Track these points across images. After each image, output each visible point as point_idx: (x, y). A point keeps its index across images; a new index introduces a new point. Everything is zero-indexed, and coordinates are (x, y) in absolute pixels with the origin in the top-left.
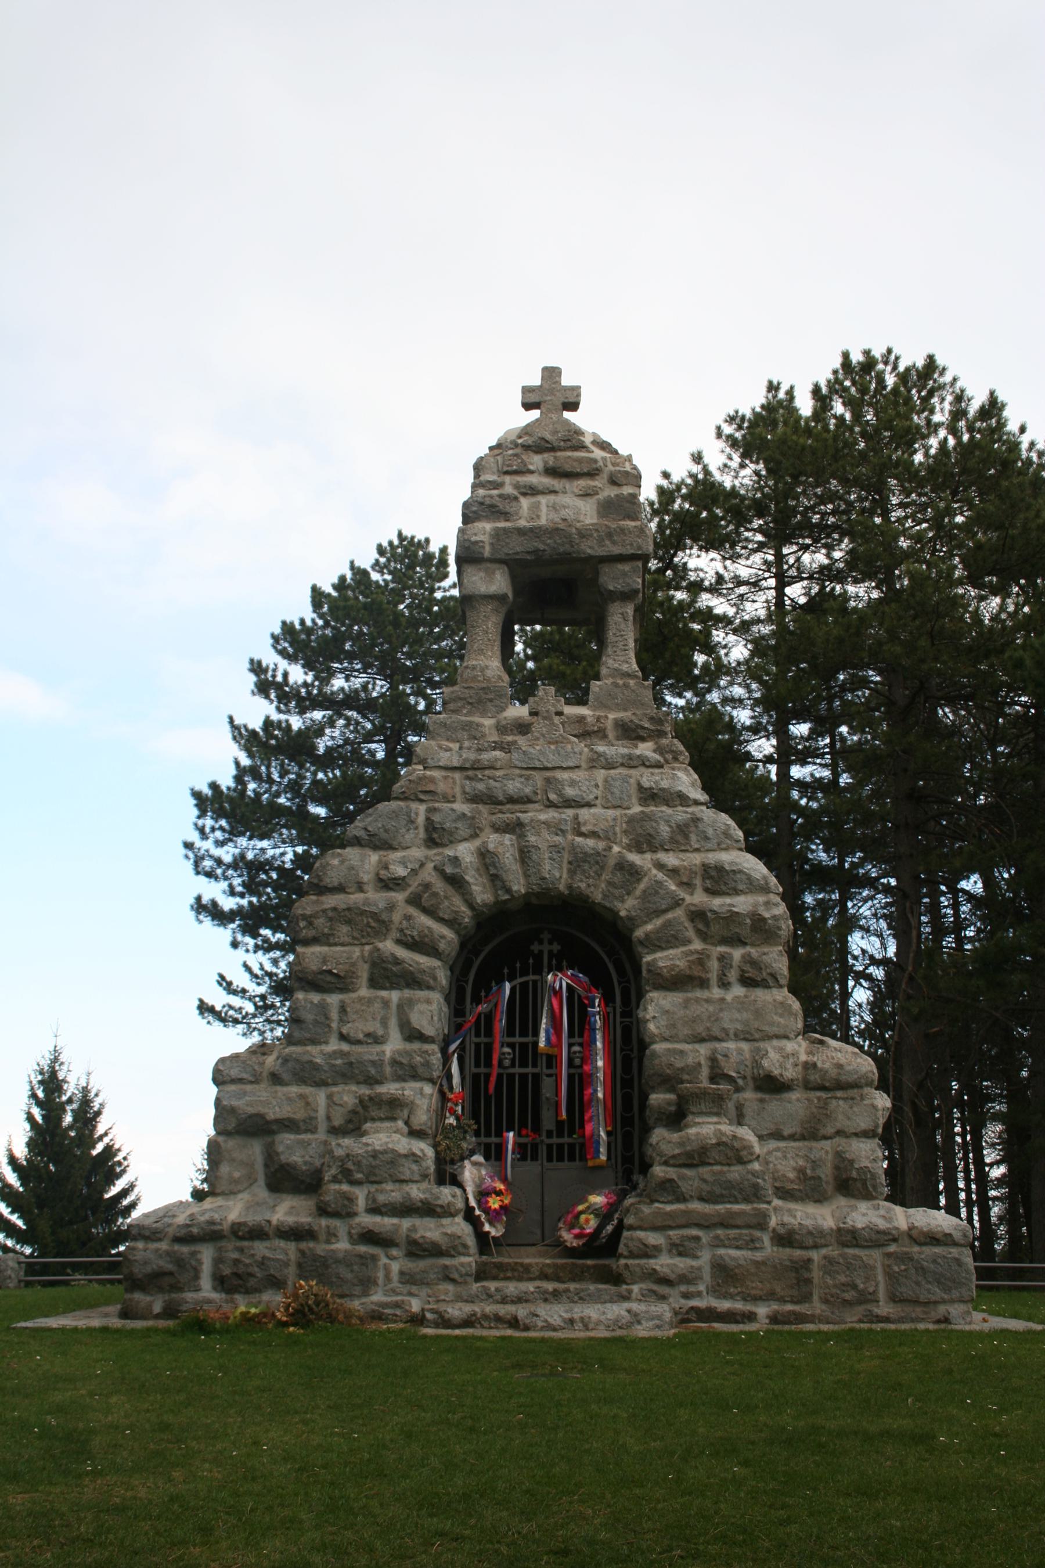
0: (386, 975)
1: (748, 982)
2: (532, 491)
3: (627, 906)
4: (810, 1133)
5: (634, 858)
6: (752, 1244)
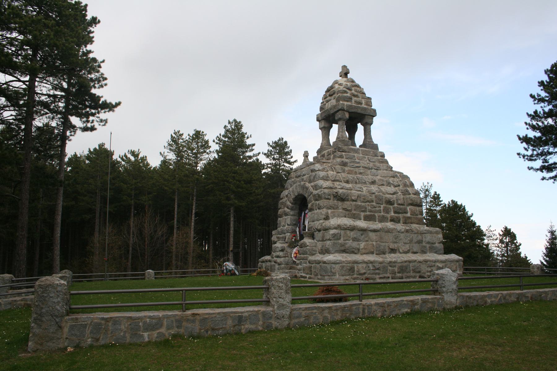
0: (286, 214)
1: (319, 209)
2: (327, 101)
3: (306, 196)
4: (323, 241)
5: (308, 185)
6: (306, 263)
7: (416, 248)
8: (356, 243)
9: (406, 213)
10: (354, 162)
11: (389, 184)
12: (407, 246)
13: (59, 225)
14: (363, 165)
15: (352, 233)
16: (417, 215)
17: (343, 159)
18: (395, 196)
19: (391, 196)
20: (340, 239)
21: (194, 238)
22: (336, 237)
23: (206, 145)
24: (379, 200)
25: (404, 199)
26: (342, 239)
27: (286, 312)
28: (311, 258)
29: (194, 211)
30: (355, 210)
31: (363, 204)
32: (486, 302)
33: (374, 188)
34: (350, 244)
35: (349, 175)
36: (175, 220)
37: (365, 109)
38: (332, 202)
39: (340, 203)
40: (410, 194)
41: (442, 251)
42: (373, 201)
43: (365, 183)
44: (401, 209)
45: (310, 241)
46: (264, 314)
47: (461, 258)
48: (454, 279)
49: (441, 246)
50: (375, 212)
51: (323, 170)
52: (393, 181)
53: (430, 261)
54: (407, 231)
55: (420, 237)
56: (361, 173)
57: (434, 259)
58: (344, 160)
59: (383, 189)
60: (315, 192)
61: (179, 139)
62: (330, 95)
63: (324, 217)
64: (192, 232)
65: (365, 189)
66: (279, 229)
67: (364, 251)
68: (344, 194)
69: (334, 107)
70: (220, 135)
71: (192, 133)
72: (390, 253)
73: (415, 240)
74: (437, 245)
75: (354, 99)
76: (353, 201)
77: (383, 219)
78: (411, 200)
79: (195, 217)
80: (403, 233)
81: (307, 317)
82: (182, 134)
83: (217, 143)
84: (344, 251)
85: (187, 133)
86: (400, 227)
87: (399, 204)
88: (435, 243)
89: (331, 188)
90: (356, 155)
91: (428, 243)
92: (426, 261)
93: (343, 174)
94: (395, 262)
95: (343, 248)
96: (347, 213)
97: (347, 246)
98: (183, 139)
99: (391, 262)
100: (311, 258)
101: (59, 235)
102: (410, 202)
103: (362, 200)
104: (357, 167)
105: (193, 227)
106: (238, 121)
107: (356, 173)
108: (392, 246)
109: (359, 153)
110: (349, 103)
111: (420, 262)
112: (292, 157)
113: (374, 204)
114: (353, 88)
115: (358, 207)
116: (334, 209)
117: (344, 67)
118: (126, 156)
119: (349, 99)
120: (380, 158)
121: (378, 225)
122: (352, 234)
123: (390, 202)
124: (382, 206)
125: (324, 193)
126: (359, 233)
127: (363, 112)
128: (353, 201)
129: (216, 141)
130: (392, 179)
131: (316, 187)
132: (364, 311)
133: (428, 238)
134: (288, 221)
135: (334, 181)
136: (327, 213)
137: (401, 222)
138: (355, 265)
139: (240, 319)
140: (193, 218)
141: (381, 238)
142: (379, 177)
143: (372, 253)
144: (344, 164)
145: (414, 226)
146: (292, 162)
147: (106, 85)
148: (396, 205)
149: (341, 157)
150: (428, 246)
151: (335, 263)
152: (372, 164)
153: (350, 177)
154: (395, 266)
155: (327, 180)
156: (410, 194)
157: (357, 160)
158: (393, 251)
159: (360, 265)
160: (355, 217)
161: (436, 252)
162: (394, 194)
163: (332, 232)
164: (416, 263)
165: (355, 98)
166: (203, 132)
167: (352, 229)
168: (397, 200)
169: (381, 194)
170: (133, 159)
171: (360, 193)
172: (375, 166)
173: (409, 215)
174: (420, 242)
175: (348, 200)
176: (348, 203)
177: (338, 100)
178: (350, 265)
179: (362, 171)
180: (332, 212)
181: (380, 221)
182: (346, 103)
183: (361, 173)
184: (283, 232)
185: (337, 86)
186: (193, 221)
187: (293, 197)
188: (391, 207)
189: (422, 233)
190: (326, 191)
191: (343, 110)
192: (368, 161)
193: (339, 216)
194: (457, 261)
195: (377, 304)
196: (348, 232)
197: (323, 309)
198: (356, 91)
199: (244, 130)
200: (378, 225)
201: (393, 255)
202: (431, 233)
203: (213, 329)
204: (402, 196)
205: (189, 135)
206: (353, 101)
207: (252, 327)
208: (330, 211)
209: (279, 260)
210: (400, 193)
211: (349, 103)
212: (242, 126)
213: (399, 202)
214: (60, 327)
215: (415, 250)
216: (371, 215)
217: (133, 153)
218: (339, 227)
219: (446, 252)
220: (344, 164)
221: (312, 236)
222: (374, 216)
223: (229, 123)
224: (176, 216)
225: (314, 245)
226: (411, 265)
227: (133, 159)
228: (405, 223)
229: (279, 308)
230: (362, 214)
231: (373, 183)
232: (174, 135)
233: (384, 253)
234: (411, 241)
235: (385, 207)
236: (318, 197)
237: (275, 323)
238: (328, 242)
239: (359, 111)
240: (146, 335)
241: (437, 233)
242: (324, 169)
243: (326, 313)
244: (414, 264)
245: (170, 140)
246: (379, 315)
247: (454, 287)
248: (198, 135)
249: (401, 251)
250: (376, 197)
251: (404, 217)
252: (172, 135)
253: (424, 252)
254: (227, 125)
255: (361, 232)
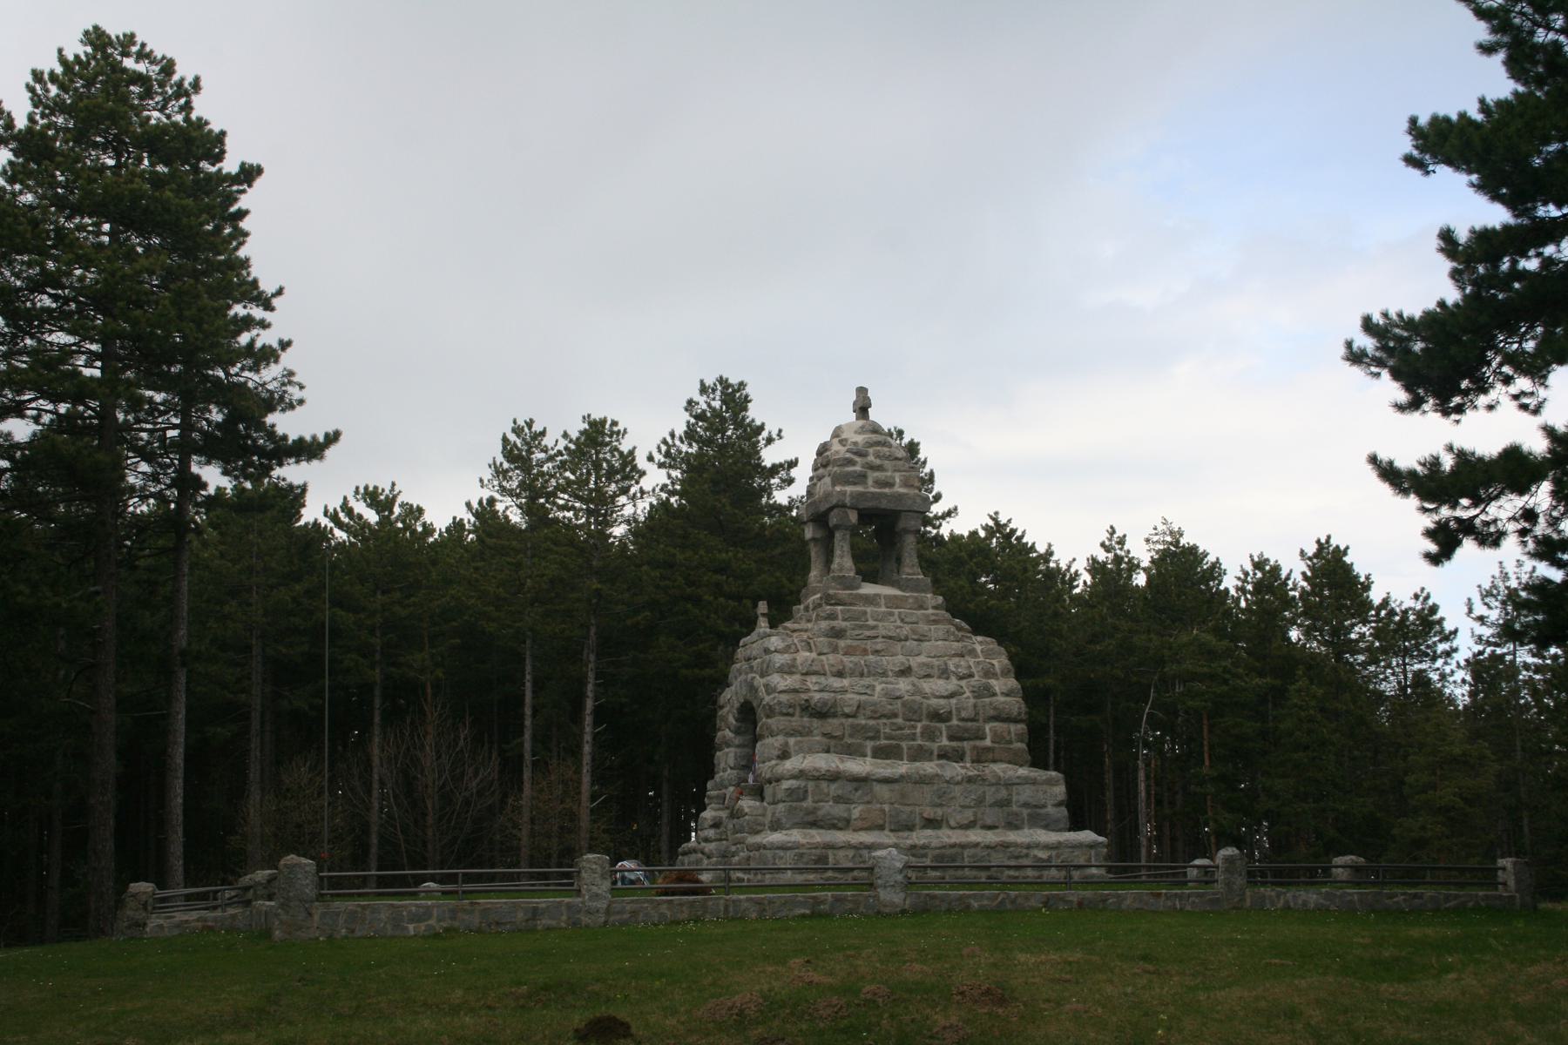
7: (990, 816)
8: (842, 807)
9: (983, 738)
10: (861, 627)
11: (945, 673)
12: (969, 815)
13: (180, 773)
14: (884, 632)
15: (833, 786)
16: (1010, 742)
17: (834, 623)
18: (954, 701)
19: (942, 702)
20: (804, 799)
21: (593, 798)
22: (797, 795)
23: (627, 469)
24: (912, 712)
25: (975, 706)
26: (810, 799)
27: (602, 905)
28: (752, 840)
29: (589, 704)
30: (851, 736)
31: (872, 722)
32: (968, 906)
33: (903, 685)
34: (828, 808)
35: (845, 659)
36: (527, 736)
37: (900, 497)
38: (797, 721)
39: (816, 723)
40: (994, 694)
41: (1065, 823)
42: (895, 715)
43: (884, 674)
44: (966, 730)
45: (752, 803)
46: (569, 906)
47: (1101, 839)
48: (899, 865)
49: (1064, 811)
50: (901, 739)
51: (786, 650)
52: (957, 666)
53: (1016, 845)
54: (970, 780)
55: (1003, 793)
56: (877, 652)
57: (1027, 840)
58: (839, 624)
59: (927, 686)
60: (767, 699)
61: (530, 452)
62: (825, 466)
63: (776, 753)
64: (586, 779)
65: (879, 688)
66: (717, 777)
67: (859, 824)
68: (825, 704)
69: (827, 495)
70: (672, 435)
71: (576, 427)
72: (924, 827)
73: (989, 799)
74: (1050, 809)
75: (872, 476)
76: (847, 716)
77: (919, 754)
78: (995, 708)
79: (596, 724)
80: (958, 783)
81: (634, 913)
82: (543, 433)
83: (661, 465)
84: (814, 824)
85: (561, 426)
86: (955, 770)
87: (963, 720)
88: (1044, 806)
89: (795, 691)
90: (868, 610)
91: (1026, 805)
92: (1005, 846)
93: (831, 657)
94: (924, 847)
95: (810, 818)
96: (833, 742)
97: (820, 813)
98: (545, 450)
99: (914, 847)
100: (752, 840)
101: (180, 800)
102: (992, 713)
103: (868, 713)
104: (869, 638)
105: (587, 759)
106: (734, 381)
107: (865, 652)
108: (929, 812)
109: (878, 605)
110: (859, 489)
111: (988, 847)
112: (938, 498)
113: (900, 721)
114: (871, 450)
115: (857, 730)
116: (801, 735)
117: (862, 391)
118: (346, 507)
119: (861, 478)
120: (931, 611)
121: (902, 768)
122: (834, 789)
123: (936, 716)
124: (919, 725)
125: (780, 703)
126: (850, 787)
127: (892, 506)
128: (847, 716)
129: (658, 457)
130: (957, 659)
131: (770, 689)
132: (726, 907)
133: (1026, 794)
134: (731, 762)
135: (807, 674)
136: (787, 744)
137: (968, 758)
138: (830, 852)
139: (535, 913)
140: (588, 729)
141: (903, 796)
142: (922, 659)
143: (881, 828)
144: (838, 634)
145: (999, 768)
146: (936, 517)
147: (301, 402)
148: (955, 722)
149: (832, 616)
150: (1025, 812)
151: (783, 847)
152: (907, 627)
153: (848, 661)
154: (925, 856)
155: (791, 673)
156: (994, 694)
157: (871, 622)
158: (932, 823)
159: (841, 853)
160: (853, 751)
161: (1046, 827)
162: (952, 696)
163: (786, 784)
164: (978, 850)
165: (877, 474)
166: (614, 423)
167: (834, 777)
168: (958, 710)
169: (918, 698)
170: (372, 517)
171: (863, 698)
172: (914, 632)
173: (988, 742)
174: (1003, 803)
175: (835, 715)
176: (835, 721)
177: (837, 480)
178: (818, 852)
179: (879, 647)
180: (796, 743)
181: (913, 759)
182: (849, 489)
183: (877, 652)
184: (722, 786)
185: (836, 447)
186: (588, 738)
187: (737, 705)
188: (943, 726)
189: (1009, 784)
190: (784, 698)
191: (844, 506)
192: (899, 623)
193: (811, 751)
194: (1093, 846)
195: (748, 900)
196: (824, 785)
197: (659, 903)
198: (877, 456)
199: (755, 413)
200: (902, 768)
201: (929, 832)
202: (1034, 782)
203: (498, 924)
204: (972, 701)
205: (565, 435)
206: (870, 482)
207: (554, 923)
208: (792, 741)
209: (709, 847)
210: (968, 694)
211: (859, 489)
212: (747, 400)
213: (963, 714)
214: (310, 914)
215: (989, 822)
216: (890, 746)
217: (371, 497)
218: (801, 775)
219: (1076, 825)
220: (838, 634)
221: (759, 793)
222: (898, 746)
223: (704, 389)
224: (528, 722)
225: (760, 811)
226: (966, 853)
227: (372, 517)
228: (977, 760)
229: (591, 898)
230: (870, 744)
231: (905, 672)
232: (512, 437)
233: (911, 828)
234: (980, 802)
235: (925, 728)
236: (771, 712)
237: (585, 919)
238: (781, 806)
239: (884, 504)
240: (411, 927)
241: (1050, 782)
242: (789, 647)
243: (664, 909)
244: (973, 851)
245: (500, 459)
246: (754, 915)
247: (899, 878)
248: (597, 434)
249: (952, 823)
250: (904, 705)
251: (975, 747)
252: (505, 440)
253: (1012, 825)
254: (697, 397)
255: (855, 784)
